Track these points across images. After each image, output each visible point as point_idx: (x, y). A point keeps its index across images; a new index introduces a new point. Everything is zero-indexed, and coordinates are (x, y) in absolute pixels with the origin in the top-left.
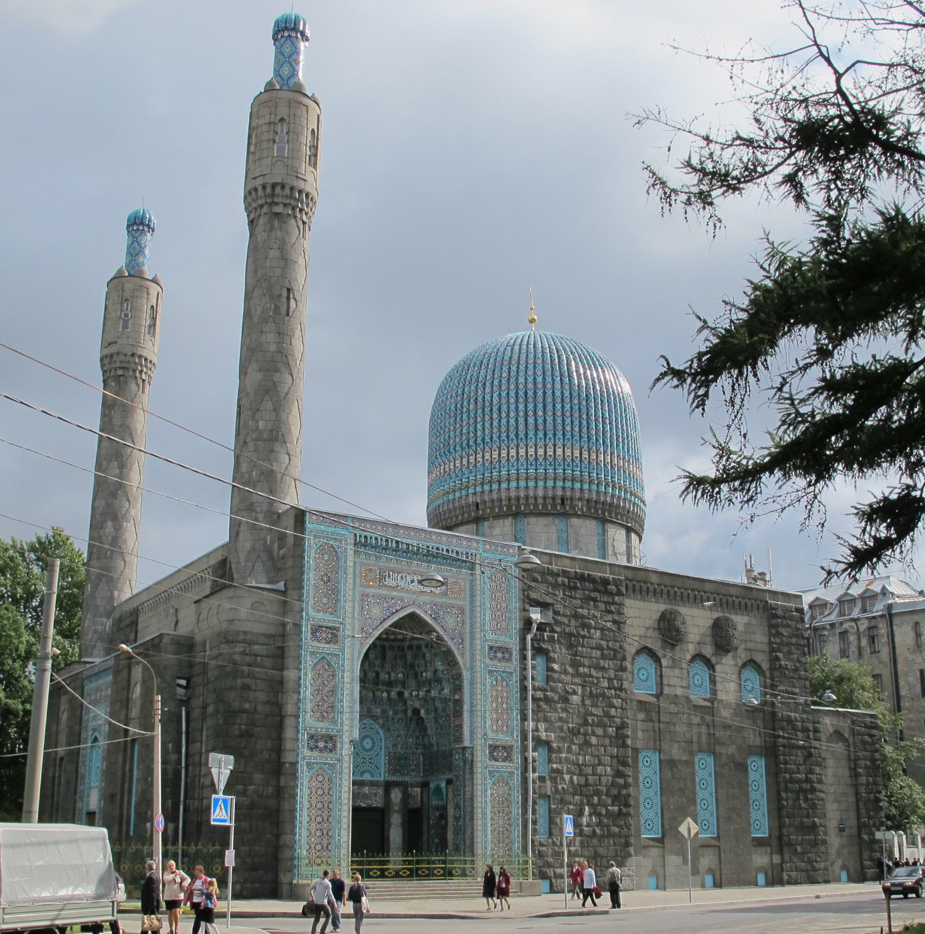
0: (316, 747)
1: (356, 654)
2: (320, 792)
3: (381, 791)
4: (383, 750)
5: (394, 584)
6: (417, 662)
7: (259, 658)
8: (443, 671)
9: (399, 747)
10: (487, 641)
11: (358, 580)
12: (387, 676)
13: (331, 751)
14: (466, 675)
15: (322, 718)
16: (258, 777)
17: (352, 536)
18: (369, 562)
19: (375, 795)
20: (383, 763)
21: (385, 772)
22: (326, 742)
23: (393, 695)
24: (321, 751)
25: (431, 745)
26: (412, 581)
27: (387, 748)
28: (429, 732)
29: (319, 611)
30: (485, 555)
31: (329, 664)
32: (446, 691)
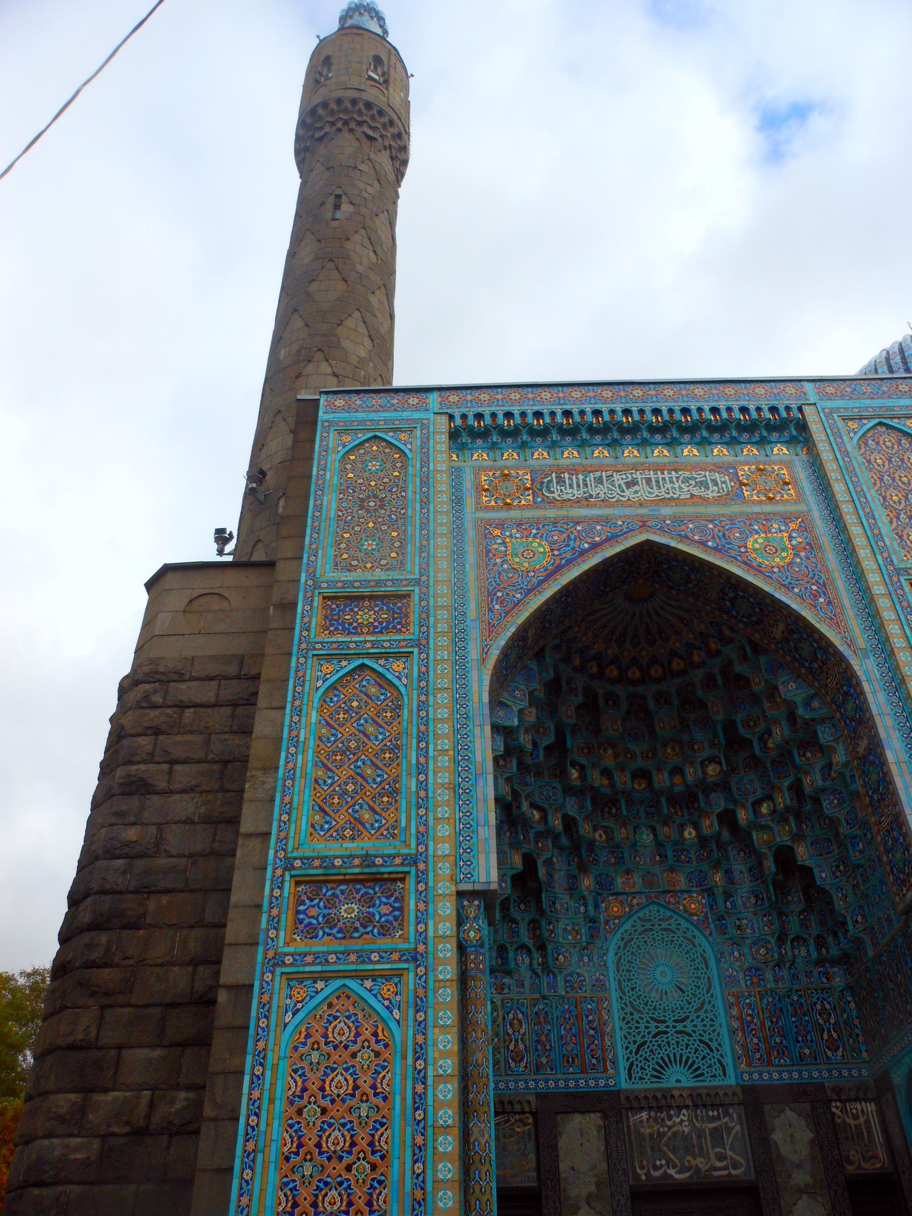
0: (330, 922)
1: (474, 653)
2: (339, 1084)
3: (734, 1123)
4: (717, 990)
5: (579, 493)
6: (739, 717)
7: (189, 712)
8: (807, 704)
9: (769, 975)
10: (899, 572)
11: (469, 502)
12: (677, 779)
13: (385, 931)
14: (866, 670)
15: (357, 827)
16: (142, 1059)
17: (444, 419)
18: (500, 463)
19: (717, 1136)
20: (724, 1031)
21: (737, 1059)
22: (369, 901)
23: (710, 825)
24: (347, 933)
25: (858, 942)
26: (631, 484)
27: (728, 981)
28: (839, 905)
29: (350, 569)
30: (830, 404)
31: (383, 682)
32: (840, 756)
